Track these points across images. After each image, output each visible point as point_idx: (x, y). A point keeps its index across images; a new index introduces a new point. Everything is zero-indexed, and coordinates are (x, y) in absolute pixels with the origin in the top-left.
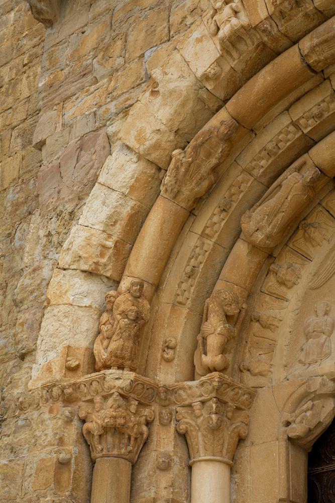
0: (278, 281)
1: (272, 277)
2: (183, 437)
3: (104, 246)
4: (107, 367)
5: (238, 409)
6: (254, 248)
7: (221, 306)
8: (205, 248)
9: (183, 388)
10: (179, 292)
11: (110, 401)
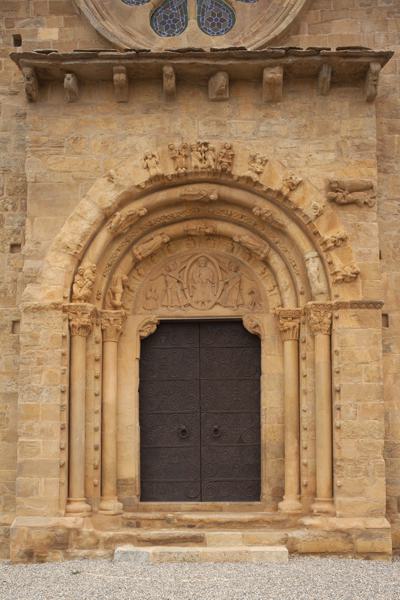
2: (102, 331)
4: (80, 299)
6: (134, 256)
11: (86, 316)
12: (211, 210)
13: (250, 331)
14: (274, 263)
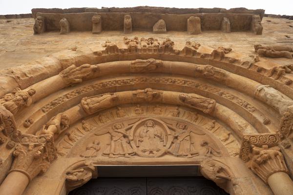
0: (83, 127)
1: (81, 124)
2: (14, 157)
3: (26, 75)
5: (47, 159)
7: (62, 119)
8: (64, 100)
9: (28, 137)
10: (45, 107)
12: (157, 79)
13: (212, 177)
14: (224, 111)
